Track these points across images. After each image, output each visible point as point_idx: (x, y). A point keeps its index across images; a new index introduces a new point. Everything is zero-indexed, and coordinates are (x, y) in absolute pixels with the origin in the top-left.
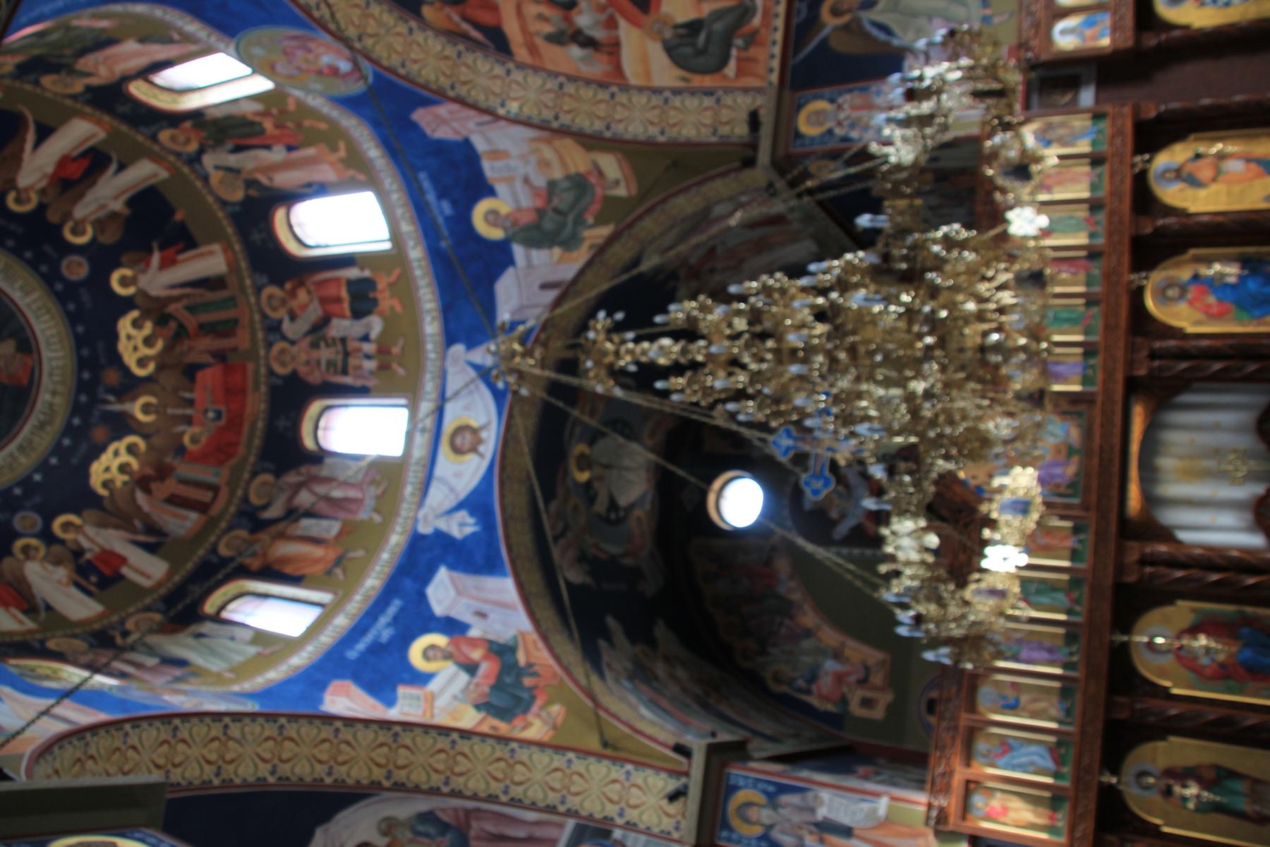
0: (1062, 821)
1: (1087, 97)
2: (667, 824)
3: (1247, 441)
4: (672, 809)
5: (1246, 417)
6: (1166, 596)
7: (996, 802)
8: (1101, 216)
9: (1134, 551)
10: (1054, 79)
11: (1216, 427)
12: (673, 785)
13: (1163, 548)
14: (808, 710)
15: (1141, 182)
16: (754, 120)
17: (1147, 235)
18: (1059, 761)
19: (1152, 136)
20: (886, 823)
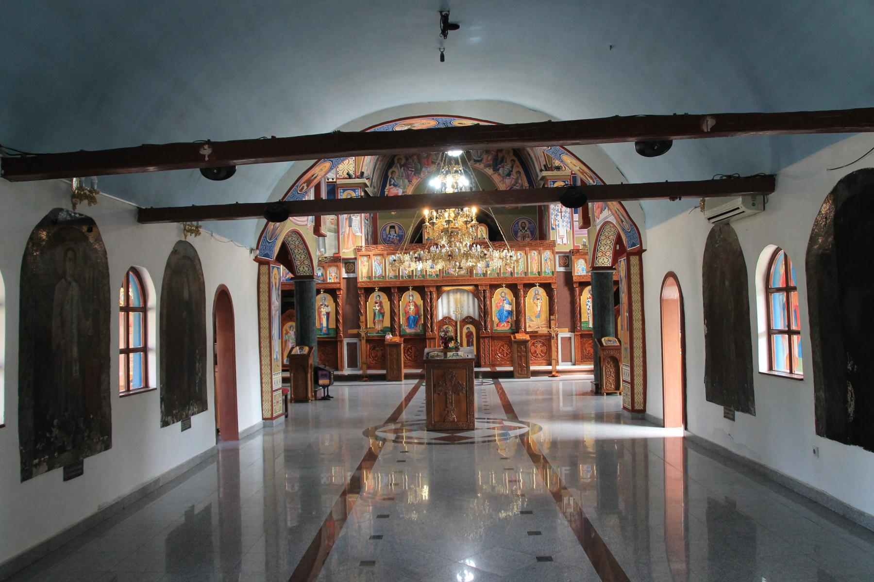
0: (364, 280)
1: (562, 269)
2: (340, 173)
3: (465, 314)
4: (345, 173)
5: (471, 314)
6: (423, 298)
7: (366, 263)
8: (523, 275)
9: (433, 290)
10: (567, 259)
11: (469, 307)
12: (351, 173)
13: (435, 296)
14: (384, 186)
15: (532, 285)
16: (558, 168)
17: (518, 288)
18: (379, 277)
19: (547, 287)
20: (355, 236)
